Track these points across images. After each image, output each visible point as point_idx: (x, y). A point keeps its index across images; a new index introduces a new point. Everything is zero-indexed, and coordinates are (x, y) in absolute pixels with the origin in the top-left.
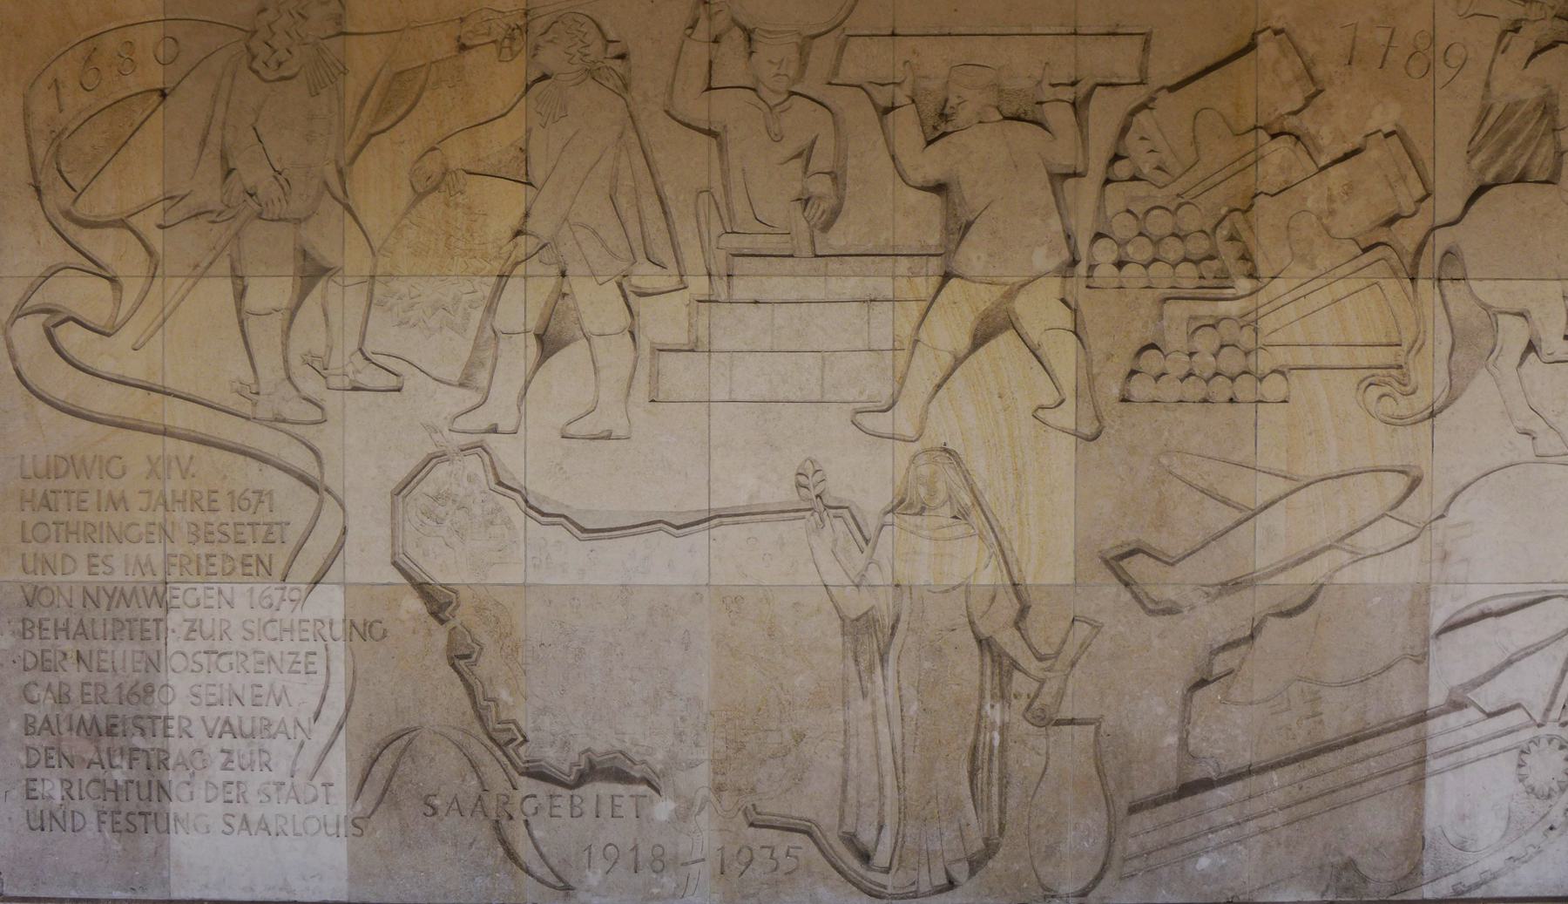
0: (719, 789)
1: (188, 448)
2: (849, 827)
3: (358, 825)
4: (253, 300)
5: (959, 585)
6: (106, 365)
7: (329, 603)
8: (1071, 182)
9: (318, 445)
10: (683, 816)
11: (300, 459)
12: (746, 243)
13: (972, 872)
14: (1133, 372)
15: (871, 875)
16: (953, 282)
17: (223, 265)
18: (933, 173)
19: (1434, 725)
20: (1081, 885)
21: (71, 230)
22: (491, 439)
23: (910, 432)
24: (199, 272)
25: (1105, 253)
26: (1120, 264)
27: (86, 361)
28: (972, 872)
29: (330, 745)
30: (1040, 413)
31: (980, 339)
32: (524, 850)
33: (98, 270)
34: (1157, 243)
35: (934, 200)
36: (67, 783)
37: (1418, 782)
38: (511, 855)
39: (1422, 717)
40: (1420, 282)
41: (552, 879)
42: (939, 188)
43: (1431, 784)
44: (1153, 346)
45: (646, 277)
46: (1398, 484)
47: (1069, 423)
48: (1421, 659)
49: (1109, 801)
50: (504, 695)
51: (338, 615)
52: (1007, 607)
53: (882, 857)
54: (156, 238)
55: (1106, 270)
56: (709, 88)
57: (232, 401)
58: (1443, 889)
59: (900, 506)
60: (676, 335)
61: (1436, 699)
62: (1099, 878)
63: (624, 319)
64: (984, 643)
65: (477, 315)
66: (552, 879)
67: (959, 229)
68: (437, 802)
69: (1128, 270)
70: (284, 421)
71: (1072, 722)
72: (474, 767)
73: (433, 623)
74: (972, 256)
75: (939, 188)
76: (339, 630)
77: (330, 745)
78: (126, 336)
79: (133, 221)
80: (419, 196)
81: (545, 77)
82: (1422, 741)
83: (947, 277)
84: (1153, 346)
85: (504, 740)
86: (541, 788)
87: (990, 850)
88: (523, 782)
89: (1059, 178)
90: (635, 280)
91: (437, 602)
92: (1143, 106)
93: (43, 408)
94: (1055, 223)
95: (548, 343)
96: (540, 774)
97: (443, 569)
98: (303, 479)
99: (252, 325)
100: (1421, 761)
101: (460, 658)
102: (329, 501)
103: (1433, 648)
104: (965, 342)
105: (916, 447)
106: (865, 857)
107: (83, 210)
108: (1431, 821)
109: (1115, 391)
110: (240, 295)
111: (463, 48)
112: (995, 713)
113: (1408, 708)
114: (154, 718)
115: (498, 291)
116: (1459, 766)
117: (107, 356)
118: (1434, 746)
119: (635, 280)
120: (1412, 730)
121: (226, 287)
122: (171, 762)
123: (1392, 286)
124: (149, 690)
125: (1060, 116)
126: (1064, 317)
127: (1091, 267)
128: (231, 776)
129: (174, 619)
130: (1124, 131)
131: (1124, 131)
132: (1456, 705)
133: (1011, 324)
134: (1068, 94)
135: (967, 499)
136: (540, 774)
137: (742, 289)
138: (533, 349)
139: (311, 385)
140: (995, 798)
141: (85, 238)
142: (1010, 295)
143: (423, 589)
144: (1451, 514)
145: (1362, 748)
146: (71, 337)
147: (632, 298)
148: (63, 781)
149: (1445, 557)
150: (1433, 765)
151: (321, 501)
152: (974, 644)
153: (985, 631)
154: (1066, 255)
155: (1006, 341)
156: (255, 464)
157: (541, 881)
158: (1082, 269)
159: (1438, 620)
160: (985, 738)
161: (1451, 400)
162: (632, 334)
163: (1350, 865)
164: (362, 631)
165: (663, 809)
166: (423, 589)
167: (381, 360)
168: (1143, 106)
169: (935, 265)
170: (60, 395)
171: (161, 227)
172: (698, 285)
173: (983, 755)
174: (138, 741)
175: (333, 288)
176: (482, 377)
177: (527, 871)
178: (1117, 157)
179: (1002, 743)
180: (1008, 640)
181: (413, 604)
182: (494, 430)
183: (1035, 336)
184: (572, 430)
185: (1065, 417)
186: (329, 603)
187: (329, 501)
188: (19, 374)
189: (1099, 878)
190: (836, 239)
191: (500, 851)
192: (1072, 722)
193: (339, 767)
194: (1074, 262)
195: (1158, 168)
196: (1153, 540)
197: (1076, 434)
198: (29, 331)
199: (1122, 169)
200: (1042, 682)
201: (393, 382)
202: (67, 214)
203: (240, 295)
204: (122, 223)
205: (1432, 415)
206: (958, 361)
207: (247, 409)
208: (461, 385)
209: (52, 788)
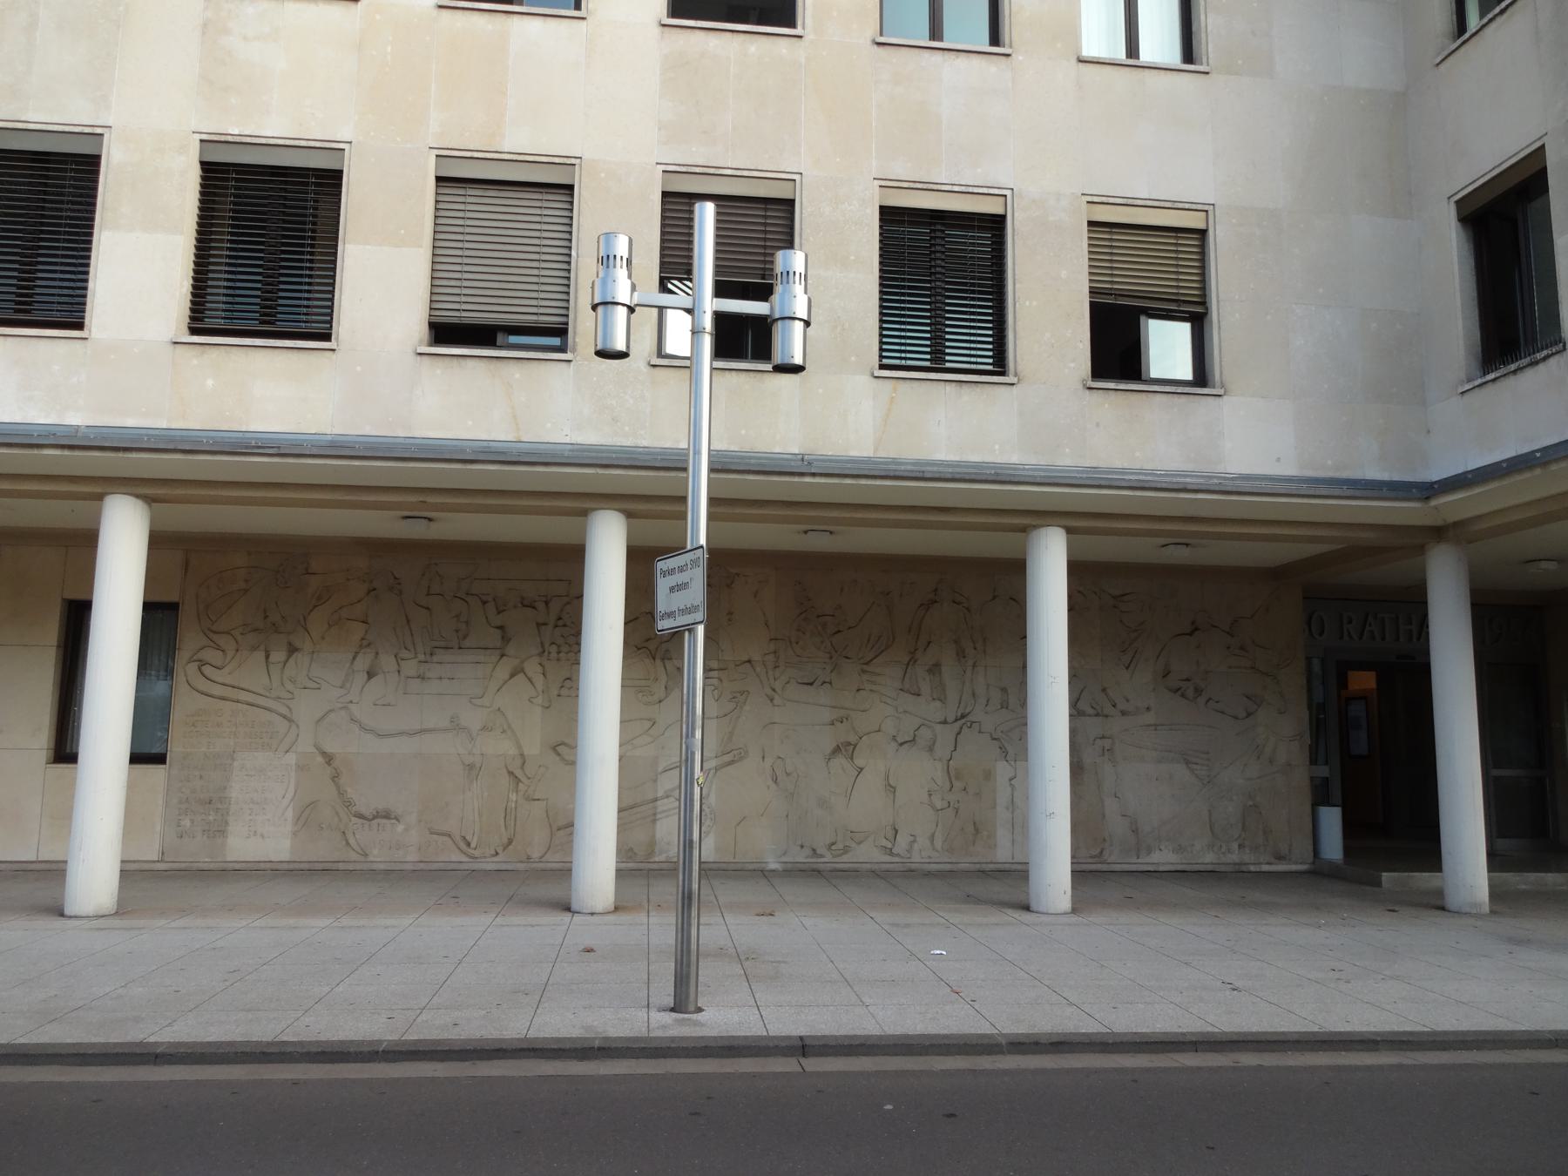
0: (420, 821)
1: (245, 706)
2: (463, 835)
3: (295, 834)
4: (272, 659)
5: (501, 755)
6: (220, 680)
7: (291, 759)
8: (543, 627)
9: (291, 706)
10: (406, 830)
11: (284, 710)
12: (436, 644)
13: (504, 850)
14: (562, 687)
15: (469, 850)
16: (505, 657)
17: (262, 647)
18: (499, 624)
19: (659, 803)
20: (540, 855)
21: (211, 635)
22: (350, 705)
23: (488, 705)
24: (254, 648)
25: (554, 649)
26: (559, 652)
27: (213, 678)
28: (504, 850)
29: (289, 805)
30: (532, 700)
31: (512, 676)
32: (352, 841)
33: (218, 648)
34: (569, 645)
35: (499, 631)
36: (192, 821)
37: (654, 821)
38: (348, 844)
39: (656, 800)
40: (656, 660)
41: (361, 852)
42: (501, 628)
43: (658, 824)
44: (568, 679)
45: (404, 654)
46: (648, 724)
47: (540, 702)
48: (655, 781)
49: (551, 826)
50: (349, 790)
51: (294, 762)
52: (518, 762)
53: (473, 845)
54: (239, 638)
55: (554, 655)
56: (428, 595)
57: (262, 692)
58: (662, 858)
59: (484, 728)
60: (413, 673)
61: (660, 794)
62: (546, 853)
63: (396, 667)
64: (511, 773)
65: (348, 665)
66: (361, 852)
67: (506, 639)
68: (324, 826)
69: (561, 655)
70: (280, 698)
71: (538, 800)
72: (337, 813)
73: (326, 765)
74: (510, 650)
75: (501, 628)
76: (294, 768)
77: (289, 805)
78: (226, 670)
79: (232, 632)
80: (330, 626)
81: (374, 589)
82: (655, 808)
83: (502, 656)
84: (568, 679)
85: (348, 804)
86: (360, 821)
87: (510, 842)
88: (353, 819)
89: (539, 625)
90: (400, 655)
91: (329, 758)
92: (568, 603)
93: (195, 692)
94: (538, 639)
95: (371, 675)
96: (361, 816)
97: (330, 748)
98: (285, 717)
99: (271, 667)
100: (655, 814)
101: (335, 778)
102: (294, 727)
103: (659, 776)
104: (507, 677)
105: (491, 709)
106: (469, 844)
107: (214, 628)
108: (658, 836)
109: (556, 693)
110: (267, 657)
111: (348, 580)
112: (513, 797)
113: (650, 796)
114: (226, 798)
115: (354, 658)
116: (667, 816)
117: (218, 676)
118: (658, 810)
119: (400, 655)
120: (651, 805)
121: (263, 654)
122: (230, 813)
123: (647, 661)
124: (225, 788)
125: (541, 606)
126: (539, 669)
127: (549, 653)
128: (251, 817)
129: (236, 764)
130: (562, 610)
131: (562, 610)
132: (668, 797)
133: (522, 671)
134: (544, 599)
135: (505, 727)
136: (361, 816)
137: (435, 658)
138: (366, 676)
139: (289, 686)
140: (513, 824)
141: (215, 637)
142: (522, 662)
143: (324, 754)
144: (666, 734)
145: (635, 810)
146: (207, 670)
147: (399, 660)
148: (191, 820)
149: (663, 748)
150: (658, 816)
151: (290, 727)
152: (506, 774)
153: (511, 770)
154: (541, 650)
155: (521, 676)
156: (268, 712)
157: (358, 853)
158: (546, 653)
159: (660, 769)
160: (509, 804)
161: (666, 697)
162: (399, 672)
163: (631, 850)
164: (301, 768)
165: (400, 828)
166: (324, 754)
167: (314, 679)
168: (568, 603)
169: (498, 652)
170: (201, 688)
171: (242, 634)
172: (422, 657)
173: (508, 810)
174: (220, 806)
175: (300, 655)
176: (348, 685)
177: (354, 850)
178: (560, 619)
179: (516, 808)
180: (518, 773)
181: (320, 759)
182: (351, 702)
183: (530, 674)
184: (377, 703)
185: (539, 700)
186: (291, 759)
187: (294, 727)
188: (187, 682)
189: (546, 853)
190: (467, 643)
191: (344, 843)
192: (538, 800)
193: (290, 814)
194: (544, 651)
195: (572, 623)
196: (566, 741)
197: (543, 706)
198: (193, 667)
199: (560, 623)
200: (529, 786)
201: (318, 686)
202: (209, 629)
203: (267, 657)
204: (228, 633)
205: (660, 702)
206: (505, 682)
207: (268, 694)
208: (341, 687)
209: (187, 823)
